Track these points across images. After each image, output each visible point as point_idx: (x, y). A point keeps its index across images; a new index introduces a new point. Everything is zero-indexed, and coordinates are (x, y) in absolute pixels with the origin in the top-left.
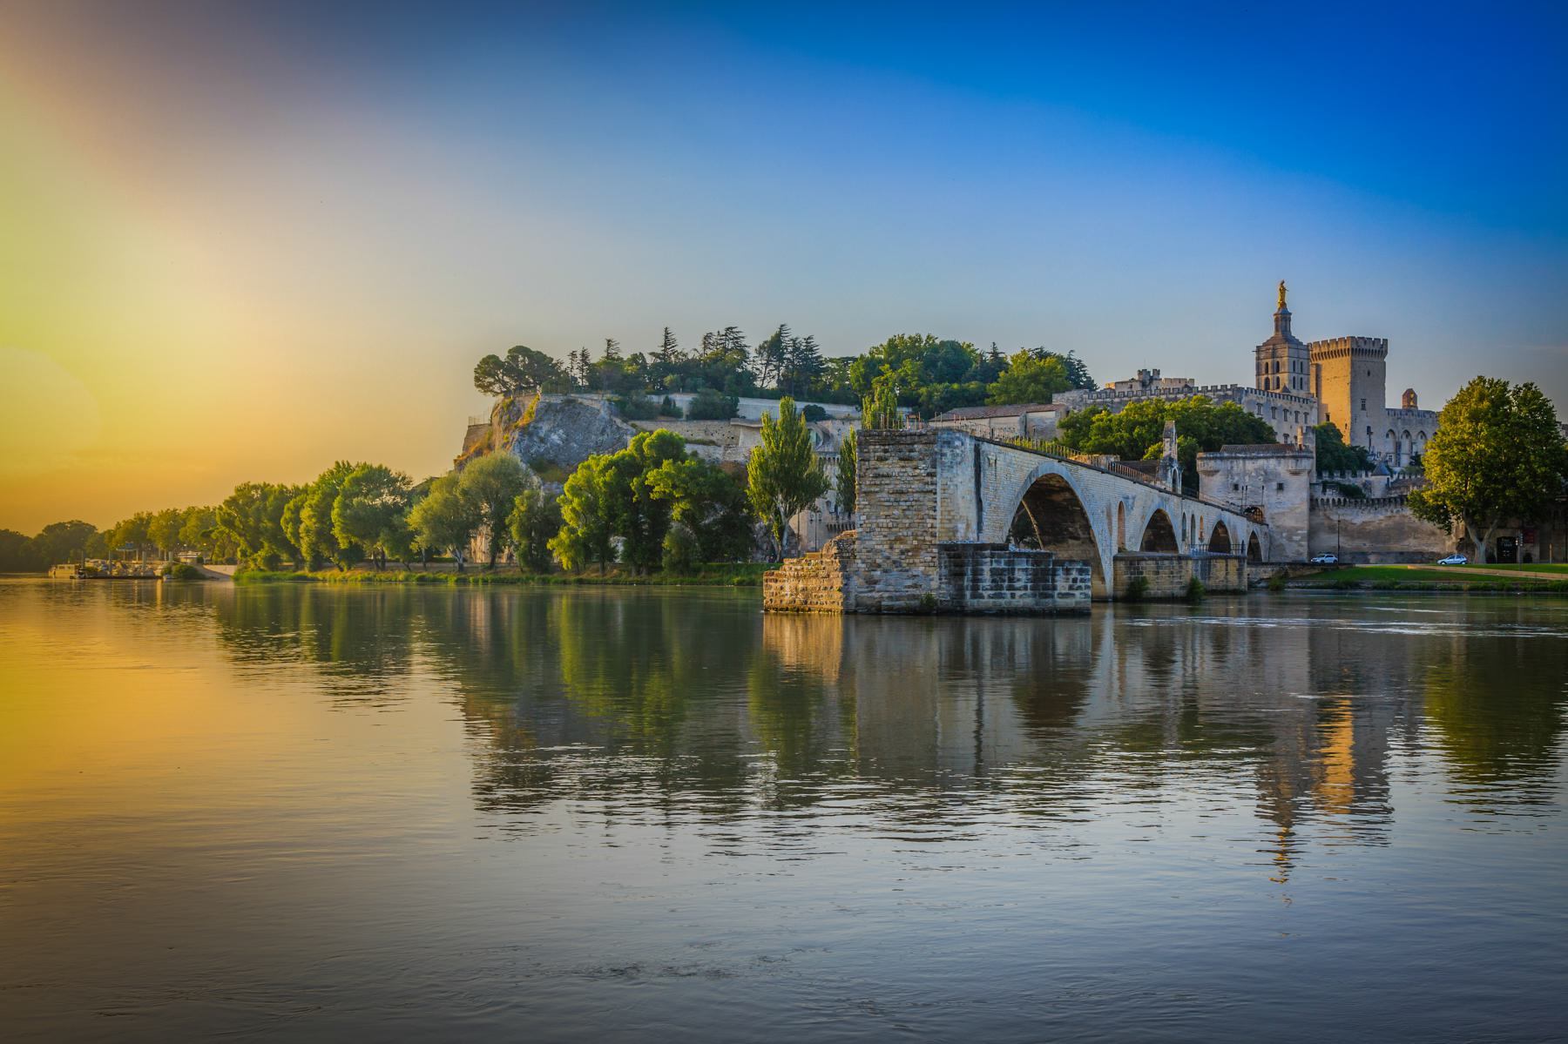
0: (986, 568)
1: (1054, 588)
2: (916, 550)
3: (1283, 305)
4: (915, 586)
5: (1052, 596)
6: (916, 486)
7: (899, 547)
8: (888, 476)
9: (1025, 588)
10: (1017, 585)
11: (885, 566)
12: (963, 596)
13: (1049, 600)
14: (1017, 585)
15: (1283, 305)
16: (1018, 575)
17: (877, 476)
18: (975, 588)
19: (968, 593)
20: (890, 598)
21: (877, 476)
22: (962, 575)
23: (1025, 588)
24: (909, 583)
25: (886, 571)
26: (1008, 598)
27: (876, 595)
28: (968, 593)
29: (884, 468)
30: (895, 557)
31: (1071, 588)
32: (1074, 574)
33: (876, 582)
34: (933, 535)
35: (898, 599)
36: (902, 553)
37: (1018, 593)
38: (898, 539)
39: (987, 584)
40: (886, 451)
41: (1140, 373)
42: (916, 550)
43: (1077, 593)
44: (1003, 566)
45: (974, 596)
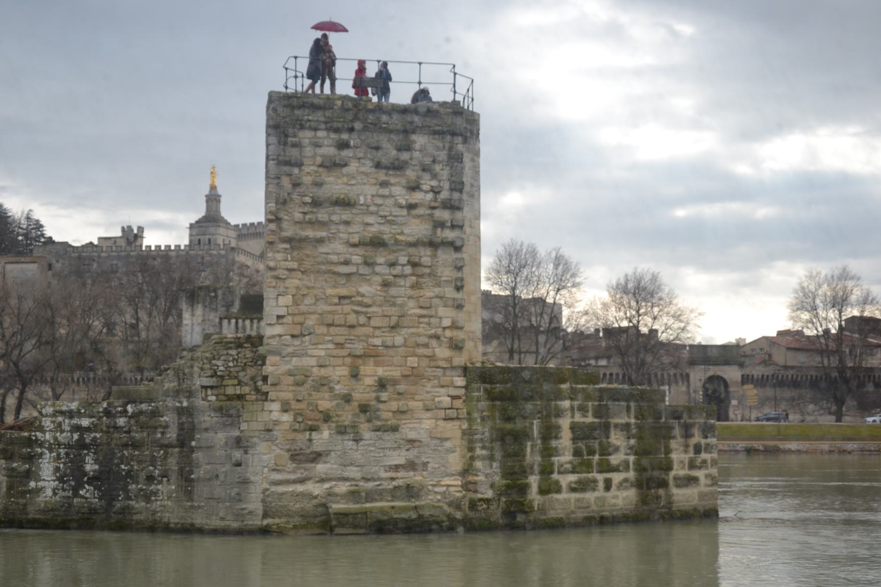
0: (565, 423)
1: (669, 468)
2: (414, 376)
3: (213, 188)
4: (411, 466)
5: (664, 484)
6: (416, 229)
7: (371, 372)
8: (345, 203)
9: (626, 466)
10: (615, 459)
11: (347, 416)
12: (523, 489)
13: (661, 492)
14: (615, 459)
15: (213, 188)
16: (616, 438)
17: (316, 203)
18: (546, 471)
19: (534, 480)
20: (354, 495)
21: (316, 203)
22: (519, 437)
23: (626, 466)
24: (399, 458)
25: (341, 431)
26: (600, 492)
27: (317, 489)
28: (534, 480)
29: (335, 185)
30: (363, 392)
31: (692, 466)
32: (697, 438)
33: (317, 457)
34: (457, 346)
35: (370, 496)
36: (382, 385)
37: (617, 478)
38: (371, 354)
39: (566, 458)
40: (343, 145)
41: (127, 231)
42: (414, 376)
43: (700, 474)
44: (590, 419)
45: (543, 492)
